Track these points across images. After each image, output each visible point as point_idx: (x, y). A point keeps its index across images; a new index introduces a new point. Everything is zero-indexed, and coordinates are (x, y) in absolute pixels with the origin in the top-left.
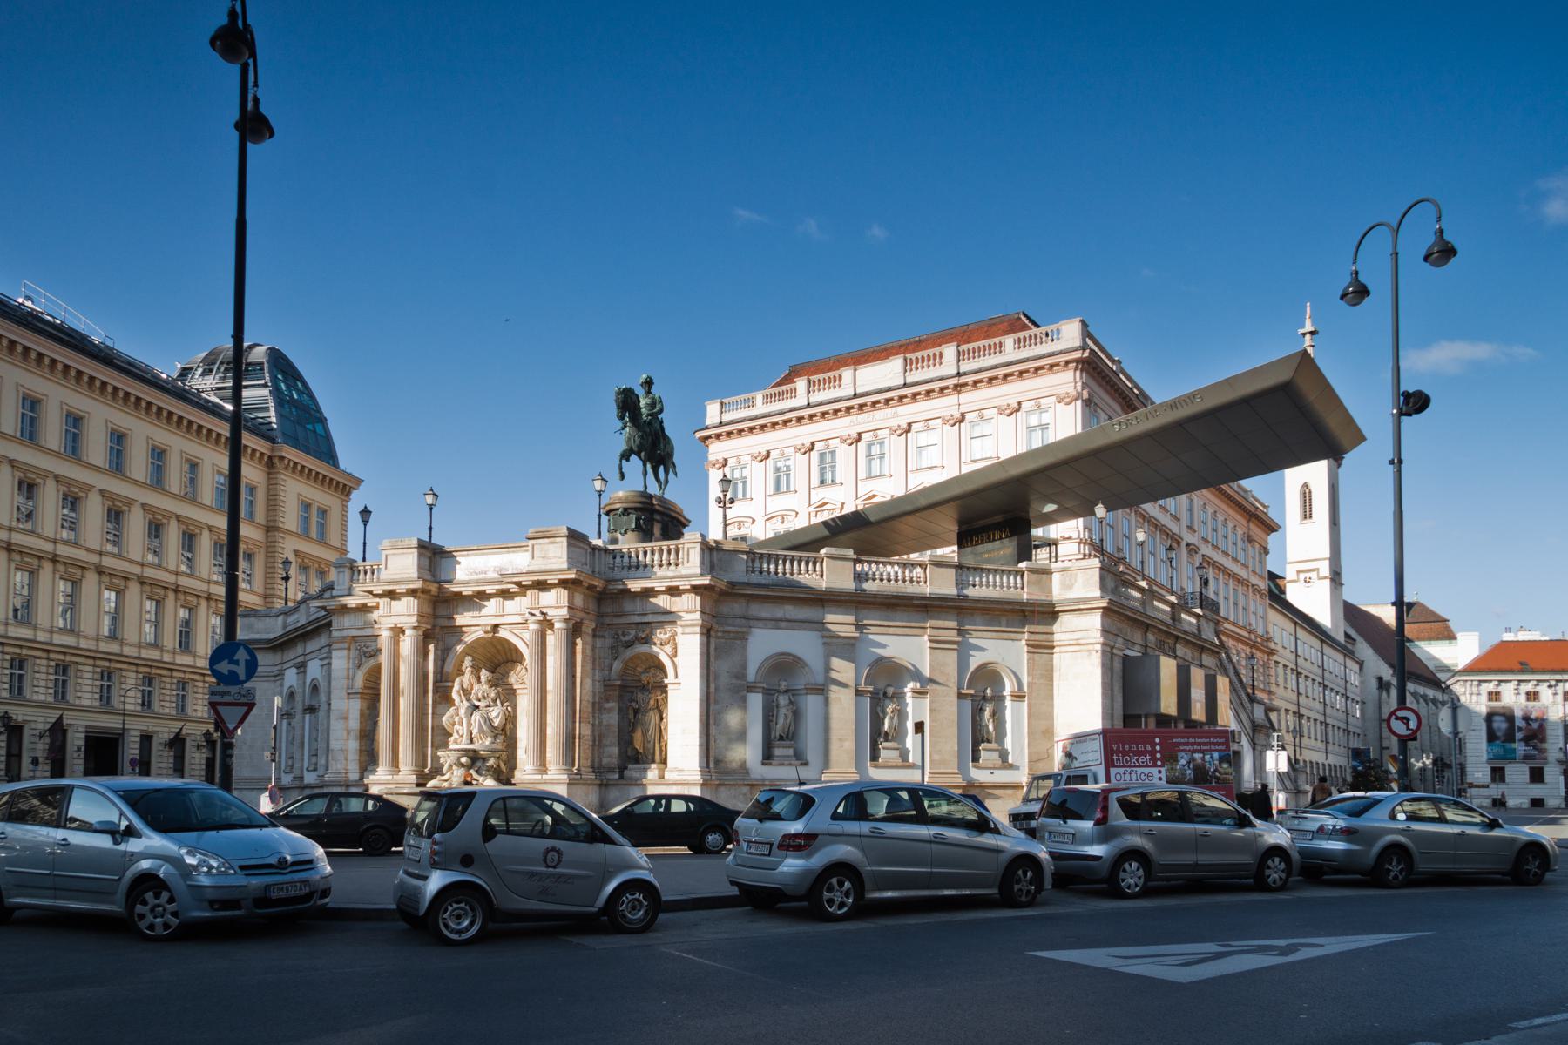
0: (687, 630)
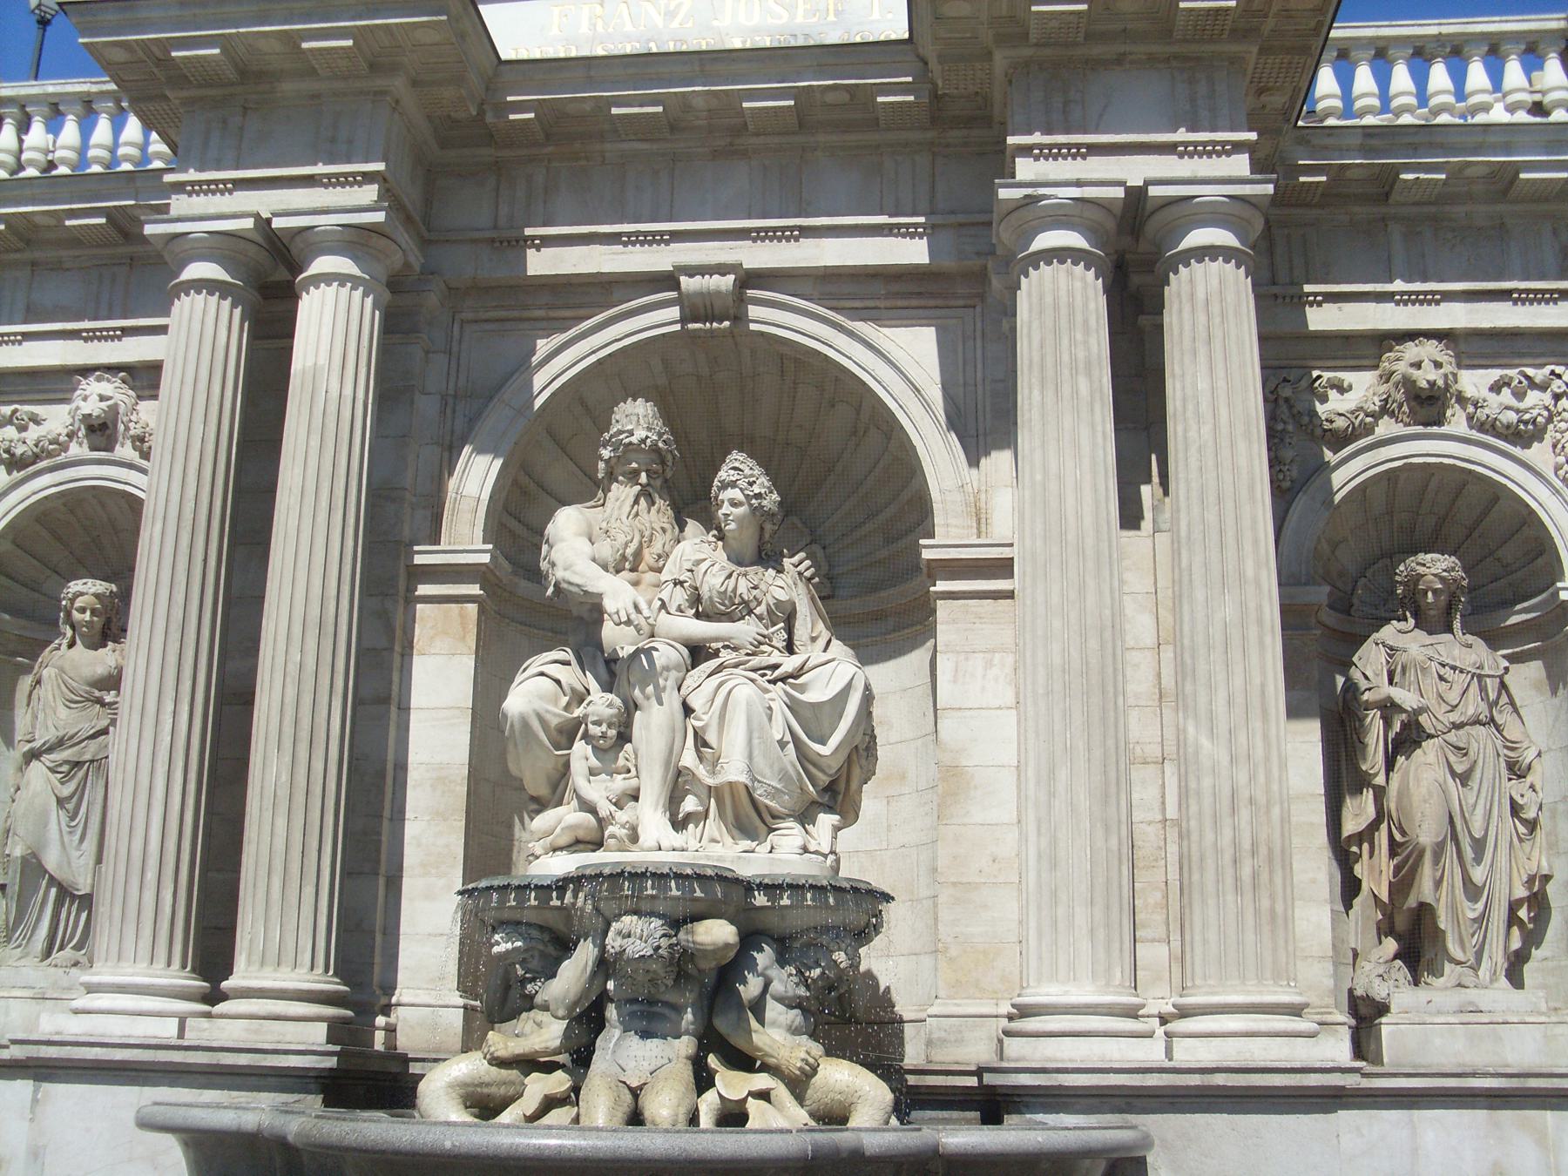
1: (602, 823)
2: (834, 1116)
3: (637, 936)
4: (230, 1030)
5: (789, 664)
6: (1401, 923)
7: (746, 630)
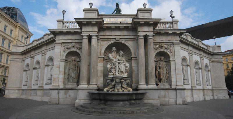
0: (176, 45)
1: (114, 74)
2: (129, 91)
3: (118, 80)
4: (90, 87)
5: (125, 64)
6: (159, 79)
7: (122, 62)
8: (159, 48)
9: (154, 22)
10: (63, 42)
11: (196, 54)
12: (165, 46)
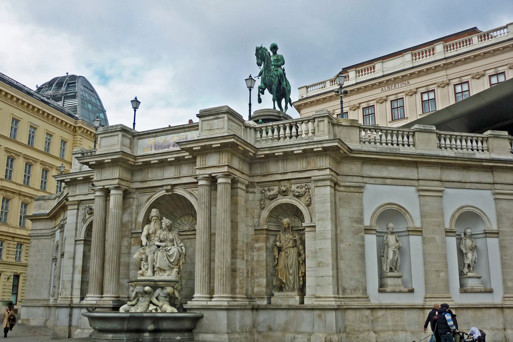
0: (320, 184)
8: (279, 197)
9: (221, 144)
10: (81, 201)
11: (467, 185)
12: (294, 187)
